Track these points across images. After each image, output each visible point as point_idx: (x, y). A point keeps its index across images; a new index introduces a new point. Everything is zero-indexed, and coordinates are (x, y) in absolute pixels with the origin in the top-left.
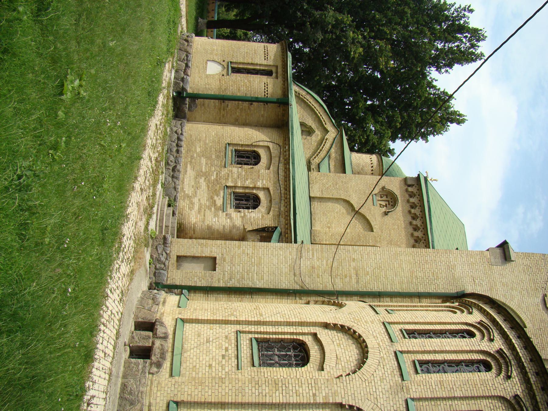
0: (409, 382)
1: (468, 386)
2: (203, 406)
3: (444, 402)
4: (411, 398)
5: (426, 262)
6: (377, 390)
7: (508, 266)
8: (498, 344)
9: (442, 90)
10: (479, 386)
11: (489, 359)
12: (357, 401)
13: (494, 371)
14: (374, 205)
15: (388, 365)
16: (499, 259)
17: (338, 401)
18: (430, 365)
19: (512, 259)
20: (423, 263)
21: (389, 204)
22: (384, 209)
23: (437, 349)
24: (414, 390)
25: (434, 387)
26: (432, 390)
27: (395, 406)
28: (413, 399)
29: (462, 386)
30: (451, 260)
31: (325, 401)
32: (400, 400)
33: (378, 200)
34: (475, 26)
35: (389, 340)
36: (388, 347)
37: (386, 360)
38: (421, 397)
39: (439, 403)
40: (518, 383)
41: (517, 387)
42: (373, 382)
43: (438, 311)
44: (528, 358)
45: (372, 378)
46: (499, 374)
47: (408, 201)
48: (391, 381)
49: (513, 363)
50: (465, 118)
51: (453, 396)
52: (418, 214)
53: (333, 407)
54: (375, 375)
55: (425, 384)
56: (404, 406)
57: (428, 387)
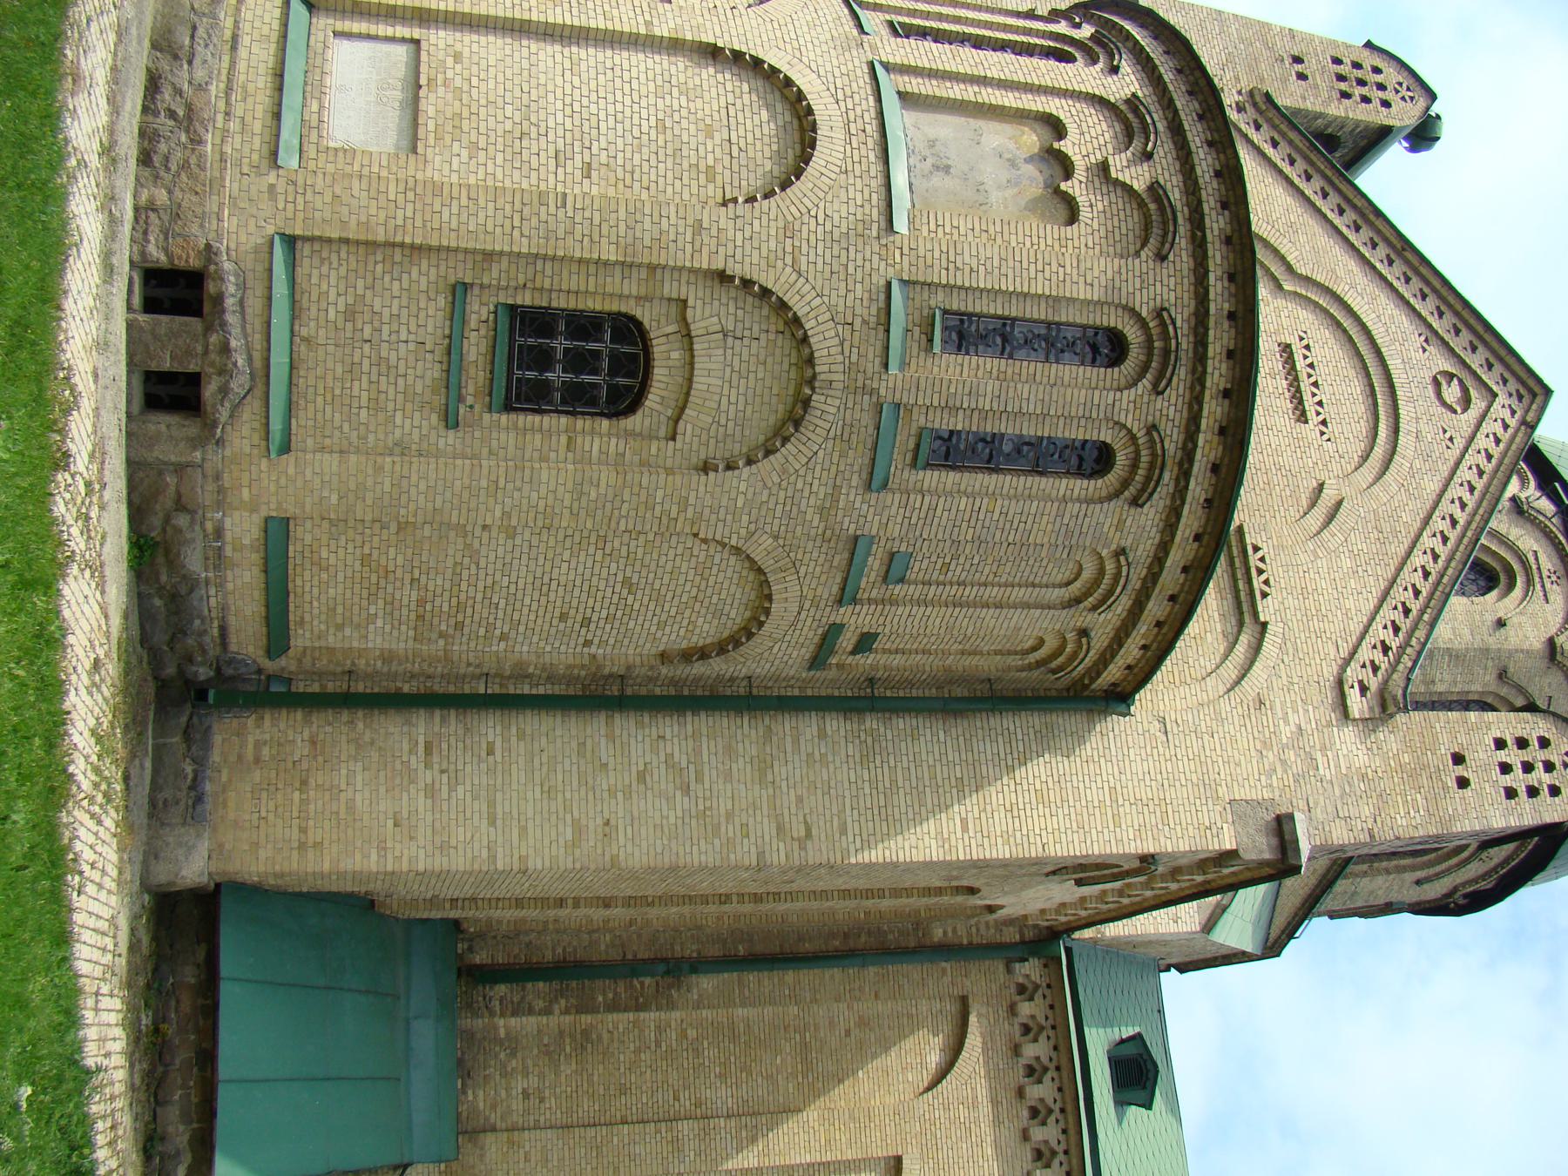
2: (373, 20)
4: (881, 62)
12: (751, 44)
17: (704, 39)
28: (887, 67)
31: (674, 35)
53: (695, 57)
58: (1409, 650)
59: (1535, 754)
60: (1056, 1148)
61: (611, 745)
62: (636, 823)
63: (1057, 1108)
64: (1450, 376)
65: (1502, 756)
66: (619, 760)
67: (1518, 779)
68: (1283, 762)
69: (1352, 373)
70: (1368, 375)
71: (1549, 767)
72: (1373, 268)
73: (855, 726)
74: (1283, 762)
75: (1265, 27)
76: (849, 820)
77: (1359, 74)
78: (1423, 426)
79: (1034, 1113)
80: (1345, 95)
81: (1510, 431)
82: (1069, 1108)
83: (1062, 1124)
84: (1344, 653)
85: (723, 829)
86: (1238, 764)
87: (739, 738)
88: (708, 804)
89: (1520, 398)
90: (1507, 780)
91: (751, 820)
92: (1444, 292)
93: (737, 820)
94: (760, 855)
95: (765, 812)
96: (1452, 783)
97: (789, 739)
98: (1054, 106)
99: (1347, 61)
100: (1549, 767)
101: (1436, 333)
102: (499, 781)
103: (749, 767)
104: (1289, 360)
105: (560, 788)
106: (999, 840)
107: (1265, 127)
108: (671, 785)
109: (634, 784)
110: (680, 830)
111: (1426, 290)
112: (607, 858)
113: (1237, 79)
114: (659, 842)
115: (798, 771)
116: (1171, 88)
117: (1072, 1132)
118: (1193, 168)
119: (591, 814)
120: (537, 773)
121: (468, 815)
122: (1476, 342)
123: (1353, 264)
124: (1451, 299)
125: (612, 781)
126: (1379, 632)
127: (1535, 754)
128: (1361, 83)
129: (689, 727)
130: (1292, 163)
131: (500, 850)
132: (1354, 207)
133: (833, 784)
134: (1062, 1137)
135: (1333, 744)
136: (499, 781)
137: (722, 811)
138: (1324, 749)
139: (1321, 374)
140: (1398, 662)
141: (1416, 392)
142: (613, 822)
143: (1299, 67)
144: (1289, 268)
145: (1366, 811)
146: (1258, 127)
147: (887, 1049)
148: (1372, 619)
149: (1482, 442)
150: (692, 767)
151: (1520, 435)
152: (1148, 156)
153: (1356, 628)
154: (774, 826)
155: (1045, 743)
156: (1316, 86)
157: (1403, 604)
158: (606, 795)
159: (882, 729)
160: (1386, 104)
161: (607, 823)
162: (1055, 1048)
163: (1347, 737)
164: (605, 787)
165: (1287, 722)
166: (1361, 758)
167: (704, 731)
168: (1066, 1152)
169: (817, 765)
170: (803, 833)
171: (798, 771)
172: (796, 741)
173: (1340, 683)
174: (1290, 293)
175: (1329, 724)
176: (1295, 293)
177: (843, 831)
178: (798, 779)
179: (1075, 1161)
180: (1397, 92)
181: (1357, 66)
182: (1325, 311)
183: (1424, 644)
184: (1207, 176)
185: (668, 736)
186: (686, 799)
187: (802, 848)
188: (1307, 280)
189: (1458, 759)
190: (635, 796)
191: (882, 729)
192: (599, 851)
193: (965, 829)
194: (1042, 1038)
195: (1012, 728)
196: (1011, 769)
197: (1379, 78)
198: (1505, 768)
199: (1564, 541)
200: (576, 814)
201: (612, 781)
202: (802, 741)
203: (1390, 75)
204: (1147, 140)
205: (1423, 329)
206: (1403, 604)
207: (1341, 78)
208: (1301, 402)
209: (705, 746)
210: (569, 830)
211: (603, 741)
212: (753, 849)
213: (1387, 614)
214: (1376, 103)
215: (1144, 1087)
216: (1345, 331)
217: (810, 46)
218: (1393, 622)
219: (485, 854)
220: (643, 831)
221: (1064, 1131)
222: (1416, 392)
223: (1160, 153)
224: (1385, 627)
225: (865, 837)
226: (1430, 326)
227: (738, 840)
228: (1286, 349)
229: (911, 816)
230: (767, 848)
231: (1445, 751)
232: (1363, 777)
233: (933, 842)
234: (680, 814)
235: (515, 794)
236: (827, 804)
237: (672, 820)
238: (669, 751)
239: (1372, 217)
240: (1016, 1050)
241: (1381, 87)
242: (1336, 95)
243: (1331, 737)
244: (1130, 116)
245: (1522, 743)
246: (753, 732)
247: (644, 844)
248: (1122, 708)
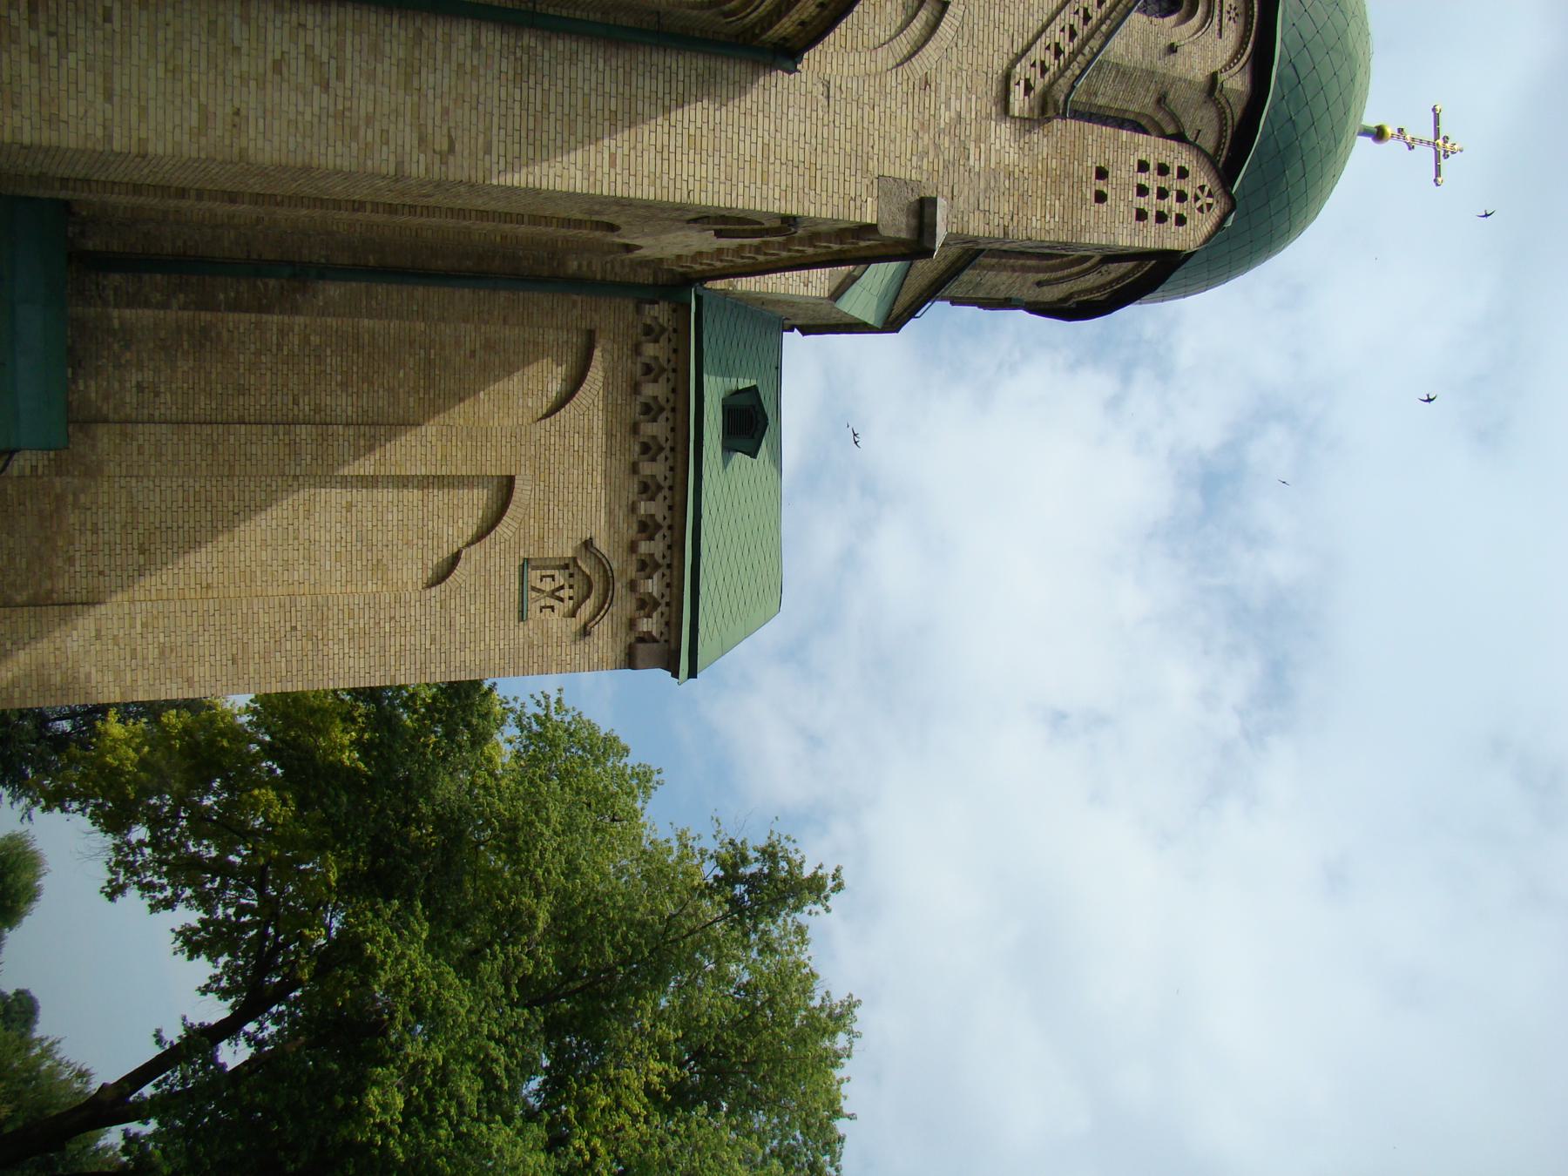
58: (1080, 58)
59: (1173, 183)
60: (662, 483)
61: (245, 28)
62: (269, 118)
63: (667, 446)
65: (1142, 178)
66: (254, 44)
67: (1151, 203)
68: (937, 146)
71: (1181, 197)
73: (512, 41)
74: (937, 146)
76: (495, 139)
79: (645, 448)
82: (679, 448)
83: (670, 462)
84: (1017, 48)
85: (362, 133)
86: (893, 141)
87: (387, 37)
88: (348, 104)
90: (1141, 202)
91: (392, 127)
93: (377, 124)
94: (399, 164)
95: (408, 121)
96: (1090, 196)
97: (440, 45)
100: (1181, 197)
102: (118, 53)
103: (394, 69)
105: (186, 69)
106: (646, 181)
108: (309, 80)
109: (269, 74)
110: (316, 130)
112: (236, 150)
114: (292, 140)
115: (446, 81)
117: (679, 470)
119: (220, 100)
120: (161, 50)
121: (81, 86)
125: (245, 68)
126: (1056, 34)
127: (1173, 183)
129: (334, 19)
131: (117, 130)
133: (482, 99)
134: (668, 474)
135: (988, 137)
136: (118, 53)
137: (363, 113)
138: (978, 140)
140: (1067, 67)
142: (243, 112)
145: (1006, 208)
147: (510, 374)
148: (1052, 19)
150: (333, 62)
153: (1034, 25)
154: (415, 136)
155: (706, 88)
157: (1086, 10)
158: (237, 82)
159: (539, 48)
161: (237, 113)
162: (674, 391)
163: (1002, 134)
164: (236, 73)
165: (948, 108)
166: (1012, 156)
167: (349, 24)
168: (671, 488)
169: (468, 77)
170: (445, 147)
171: (446, 81)
172: (448, 48)
173: (1007, 77)
175: (988, 117)
177: (488, 151)
178: (446, 89)
179: (678, 498)
183: (1096, 55)
185: (310, 25)
186: (324, 96)
187: (444, 162)
189: (1102, 174)
190: (269, 86)
191: (539, 48)
192: (227, 142)
193: (613, 164)
194: (662, 380)
195: (674, 66)
196: (667, 110)
198: (1142, 191)
200: (203, 99)
201: (245, 68)
202: (454, 50)
206: (1086, 10)
209: (349, 40)
210: (195, 116)
211: (237, 22)
212: (392, 157)
213: (1068, 17)
215: (753, 437)
218: (1071, 27)
219: (99, 132)
220: (276, 124)
221: (672, 469)
224: (1063, 30)
225: (509, 159)
227: (377, 147)
229: (559, 143)
230: (407, 158)
231: (1091, 164)
232: (1010, 175)
233: (579, 174)
234: (316, 109)
235: (134, 69)
236: (474, 120)
237: (308, 117)
238: (309, 41)
240: (636, 389)
243: (988, 129)
245: (1163, 170)
246: (403, 33)
247: (276, 143)
248: (789, 64)
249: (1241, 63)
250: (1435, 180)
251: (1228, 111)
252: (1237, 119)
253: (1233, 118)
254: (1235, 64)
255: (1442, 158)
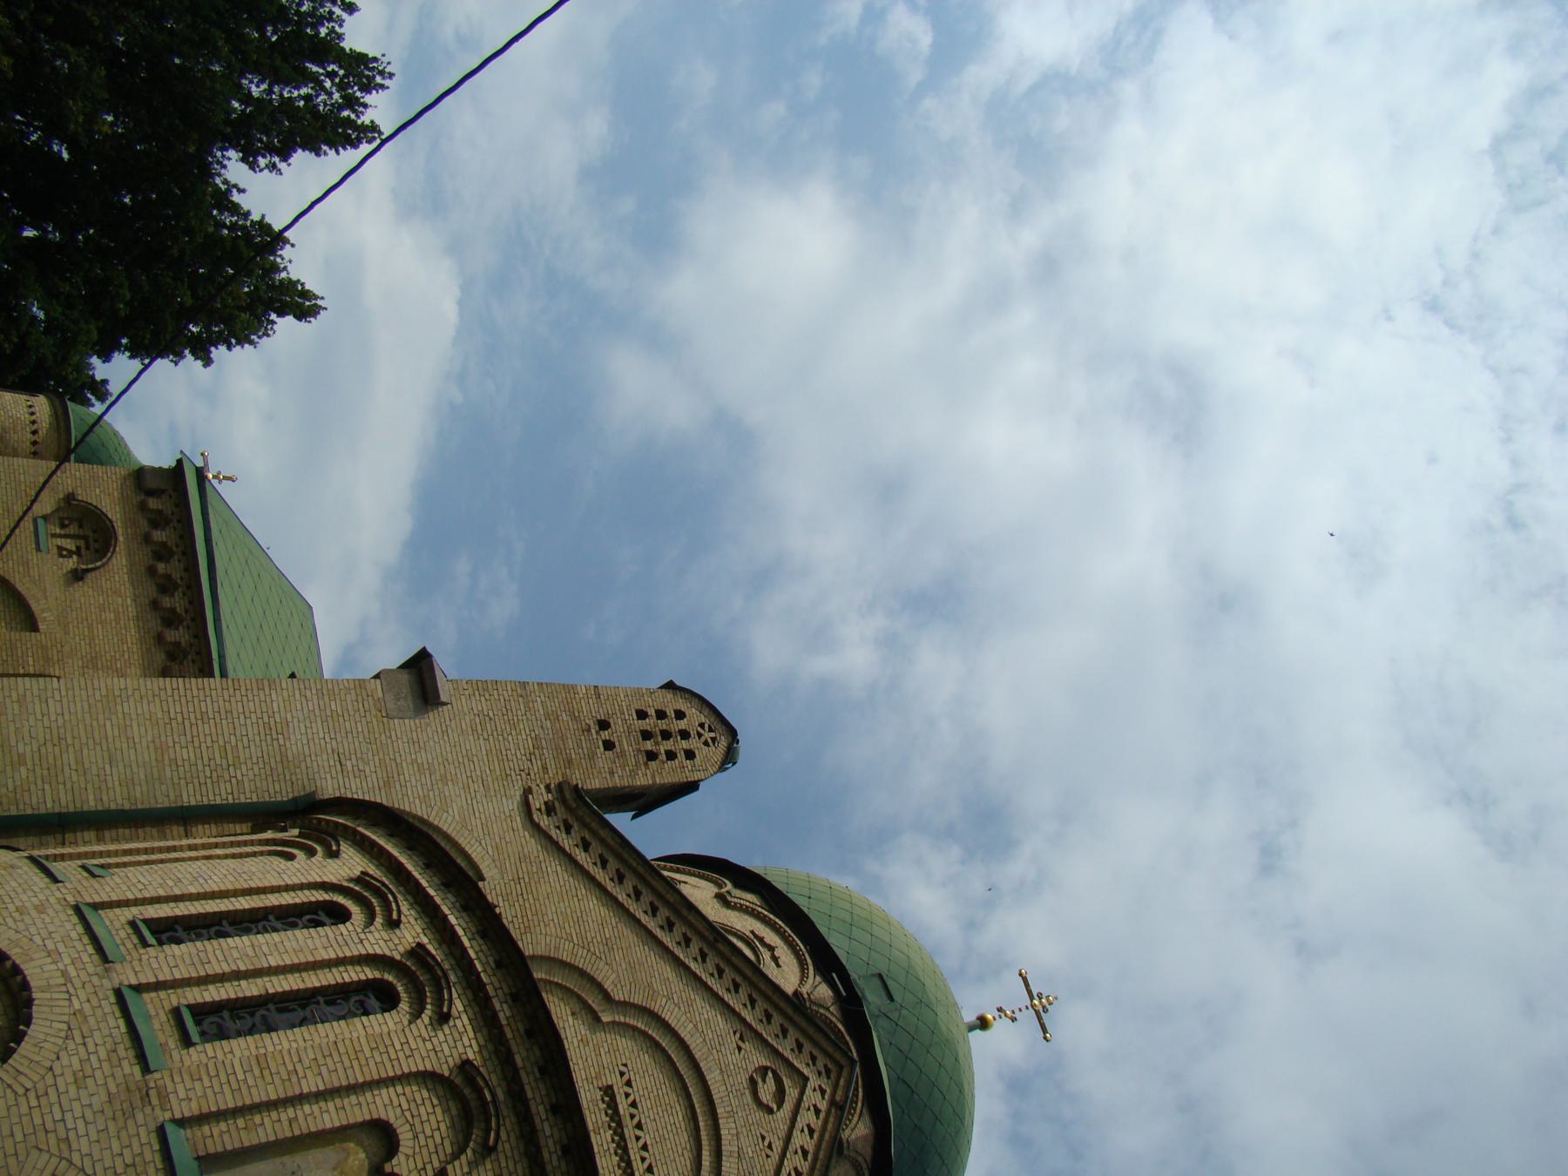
0: (166, 1074)
1: (337, 1059)
3: (274, 1115)
5: (204, 718)
6: (68, 1116)
7: (433, 717)
8: (413, 932)
9: (256, 217)
10: (368, 1054)
11: (389, 977)
13: (404, 1006)
14: (38, 549)
15: (97, 1034)
16: (408, 703)
18: (226, 1014)
19: (443, 698)
20: (193, 721)
21: (88, 548)
22: (72, 563)
23: (243, 968)
24: (182, 1094)
25: (241, 1076)
26: (235, 1086)
27: (126, 1152)
28: (181, 1123)
29: (321, 1062)
30: (276, 709)
32: (142, 1131)
33: (54, 536)
34: (360, 48)
35: (96, 958)
36: (95, 980)
37: (92, 1020)
38: (205, 1110)
39: (257, 1118)
40: (469, 1028)
41: (465, 1039)
42: (51, 1091)
43: (241, 856)
44: (491, 960)
45: (49, 1080)
46: (416, 1014)
47: (147, 539)
48: (110, 1080)
49: (453, 978)
50: (319, 302)
51: (297, 1092)
52: (176, 576)
54: (58, 1071)
55: (213, 1073)
56: (157, 1147)
57: (224, 1080)
64: (763, 1071)
69: (673, 1097)
70: (688, 1096)
72: (687, 968)
75: (570, 689)
77: (663, 725)
78: (744, 1142)
80: (651, 756)
81: (822, 1115)
89: (828, 1071)
92: (755, 979)
98: (382, 1104)
99: (652, 712)
101: (749, 1026)
104: (612, 1104)
107: (576, 826)
111: (739, 979)
113: (545, 768)
116: (509, 1035)
118: (539, 1150)
122: (786, 1025)
123: (668, 971)
124: (762, 986)
128: (666, 735)
130: (604, 863)
132: (667, 903)
139: (646, 1113)
141: (735, 1102)
143: (605, 735)
144: (607, 996)
146: (568, 829)
149: (800, 1139)
151: (831, 1119)
152: (487, 1150)
156: (623, 754)
160: (690, 755)
174: (608, 1023)
176: (614, 1022)
180: (700, 735)
181: (661, 715)
182: (644, 1034)
184: (554, 1157)
188: (626, 1006)
197: (682, 724)
199: (843, 1029)
203: (694, 717)
204: (487, 1131)
205: (738, 1026)
207: (646, 735)
208: (625, 1149)
214: (681, 756)
216: (663, 1050)
217: (80, 1124)
222: (735, 1102)
223: (505, 1147)
226: (743, 1021)
228: (608, 1091)
239: (685, 912)
241: (685, 735)
242: (642, 758)
244: (467, 1091)
249: (858, 1111)
250: (1045, 1038)
251: (860, 1159)
252: (869, 1162)
253: (866, 1161)
254: (853, 1116)
255: (1042, 1013)
